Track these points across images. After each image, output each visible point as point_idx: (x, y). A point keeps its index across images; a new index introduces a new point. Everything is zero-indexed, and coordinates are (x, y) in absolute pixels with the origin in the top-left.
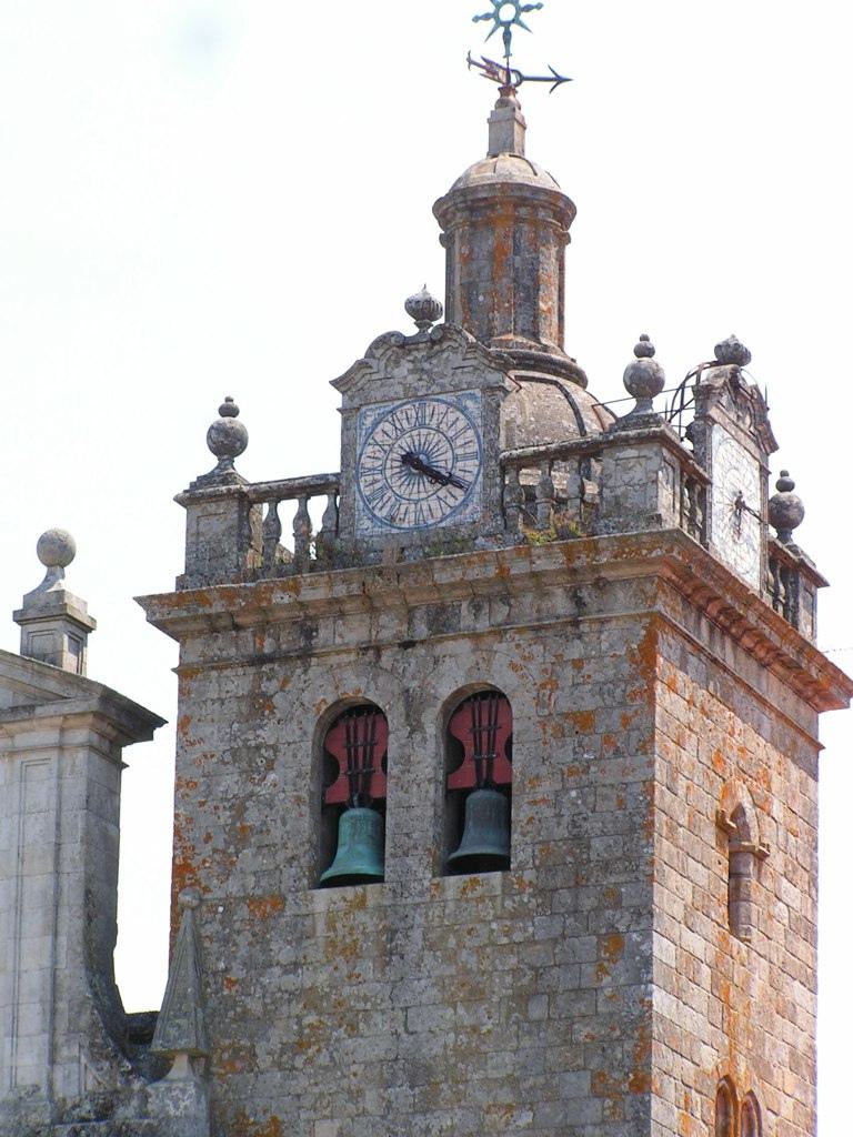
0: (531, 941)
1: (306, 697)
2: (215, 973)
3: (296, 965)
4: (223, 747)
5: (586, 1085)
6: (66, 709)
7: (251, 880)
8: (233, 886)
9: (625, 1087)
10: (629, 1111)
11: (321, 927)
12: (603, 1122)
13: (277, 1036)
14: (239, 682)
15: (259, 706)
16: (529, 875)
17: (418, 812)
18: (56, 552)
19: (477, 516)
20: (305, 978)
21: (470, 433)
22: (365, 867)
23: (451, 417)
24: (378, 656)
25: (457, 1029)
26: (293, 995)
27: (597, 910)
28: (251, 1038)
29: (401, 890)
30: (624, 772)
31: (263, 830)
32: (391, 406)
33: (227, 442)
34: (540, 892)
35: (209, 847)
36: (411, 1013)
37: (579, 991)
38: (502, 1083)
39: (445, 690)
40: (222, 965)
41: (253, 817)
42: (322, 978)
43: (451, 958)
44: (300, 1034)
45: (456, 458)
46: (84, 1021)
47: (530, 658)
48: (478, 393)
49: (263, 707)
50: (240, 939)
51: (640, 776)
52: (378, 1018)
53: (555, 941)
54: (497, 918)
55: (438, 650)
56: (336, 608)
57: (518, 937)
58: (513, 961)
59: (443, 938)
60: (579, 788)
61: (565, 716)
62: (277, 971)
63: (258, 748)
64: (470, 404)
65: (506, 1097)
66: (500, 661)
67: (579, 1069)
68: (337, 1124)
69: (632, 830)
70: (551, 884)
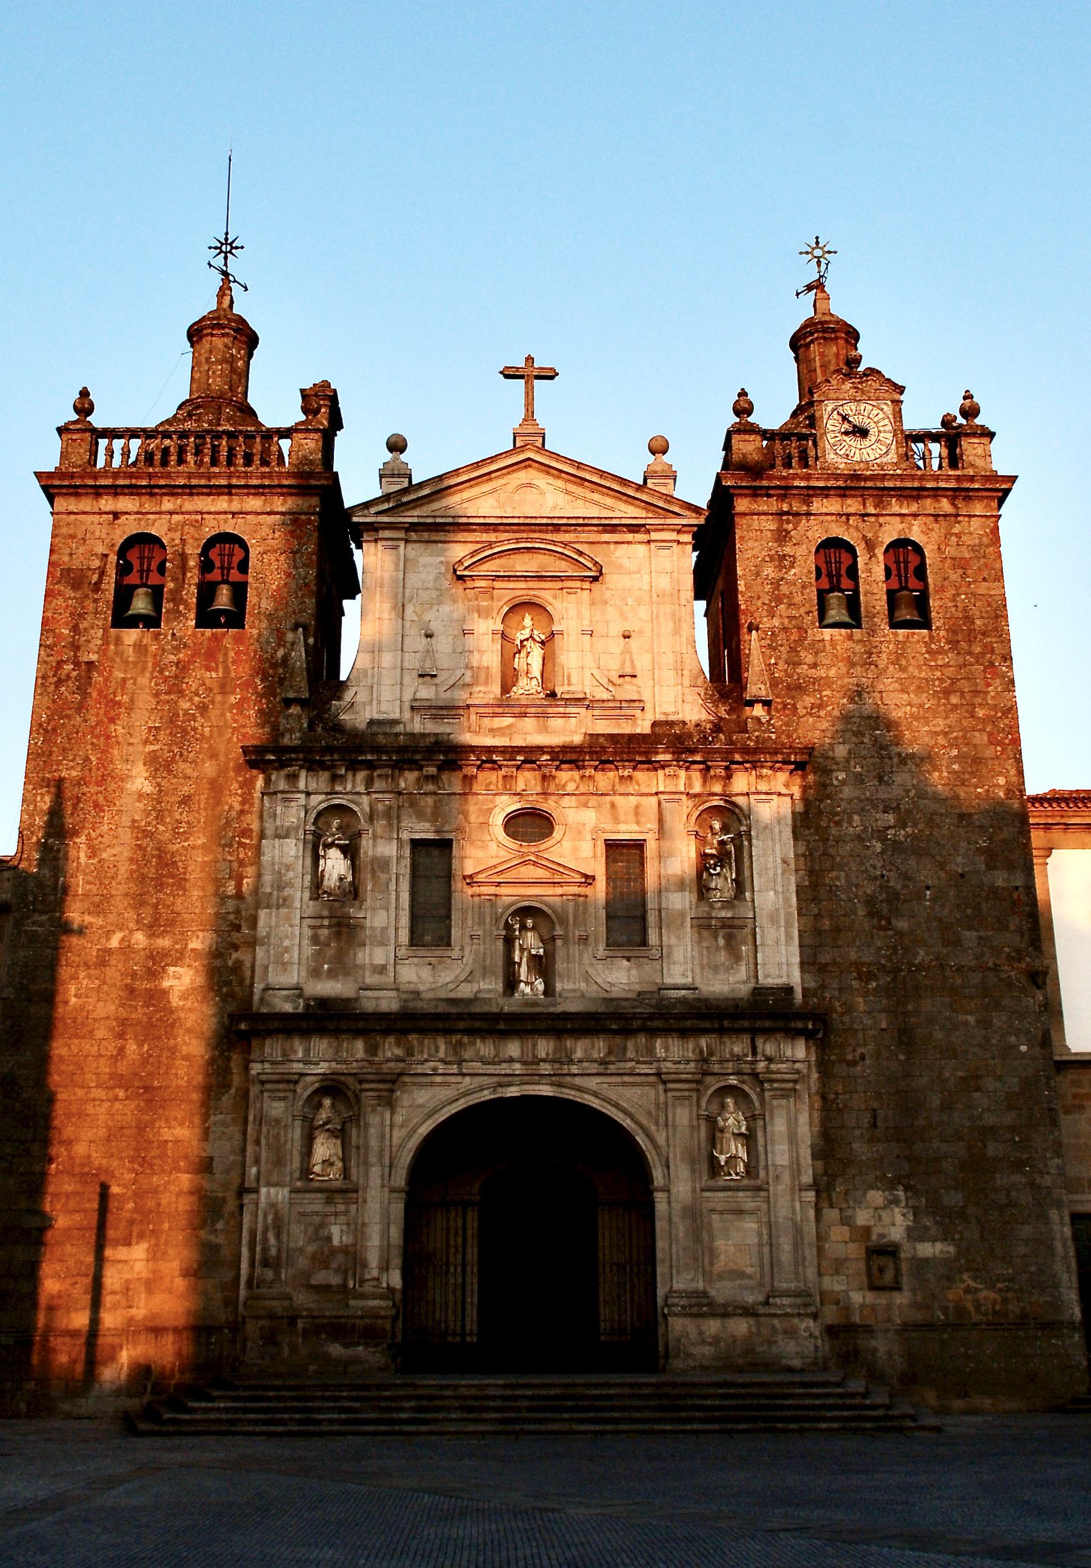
0: (947, 665)
1: (809, 534)
2: (770, 664)
3: (814, 666)
4: (764, 553)
5: (986, 739)
6: (685, 522)
7: (786, 621)
8: (776, 622)
9: (1007, 741)
10: (1011, 755)
11: (828, 648)
12: (997, 757)
13: (808, 700)
14: (770, 524)
15: (782, 536)
16: (942, 633)
17: (877, 597)
18: (659, 448)
19: (895, 460)
20: (821, 672)
21: (886, 421)
22: (847, 619)
23: (875, 412)
24: (848, 520)
25: (910, 704)
26: (815, 681)
27: (983, 654)
28: (793, 698)
29: (872, 632)
30: (989, 588)
31: (790, 596)
32: (841, 403)
33: (743, 408)
34: (948, 642)
35: (759, 603)
36: (884, 695)
37: (976, 693)
38: (936, 733)
39: (888, 541)
40: (773, 661)
41: (784, 589)
42: (832, 673)
43: (903, 669)
44: (821, 698)
45: (879, 432)
46: (700, 682)
47: (932, 530)
48: (889, 402)
49: (785, 536)
50: (782, 649)
51: (997, 592)
52: (865, 695)
53: (960, 667)
54: (927, 652)
55: (881, 520)
56: (824, 492)
57: (940, 663)
58: (938, 674)
59: (898, 659)
60: (966, 594)
61: (953, 559)
62: (805, 667)
63: (784, 556)
64: (884, 407)
65: (941, 740)
66: (915, 528)
67: (980, 730)
68: (847, 747)
69: (997, 617)
70: (956, 638)
